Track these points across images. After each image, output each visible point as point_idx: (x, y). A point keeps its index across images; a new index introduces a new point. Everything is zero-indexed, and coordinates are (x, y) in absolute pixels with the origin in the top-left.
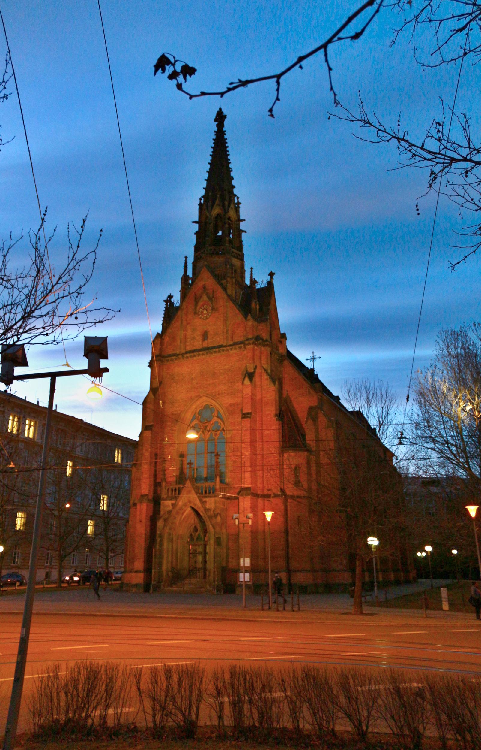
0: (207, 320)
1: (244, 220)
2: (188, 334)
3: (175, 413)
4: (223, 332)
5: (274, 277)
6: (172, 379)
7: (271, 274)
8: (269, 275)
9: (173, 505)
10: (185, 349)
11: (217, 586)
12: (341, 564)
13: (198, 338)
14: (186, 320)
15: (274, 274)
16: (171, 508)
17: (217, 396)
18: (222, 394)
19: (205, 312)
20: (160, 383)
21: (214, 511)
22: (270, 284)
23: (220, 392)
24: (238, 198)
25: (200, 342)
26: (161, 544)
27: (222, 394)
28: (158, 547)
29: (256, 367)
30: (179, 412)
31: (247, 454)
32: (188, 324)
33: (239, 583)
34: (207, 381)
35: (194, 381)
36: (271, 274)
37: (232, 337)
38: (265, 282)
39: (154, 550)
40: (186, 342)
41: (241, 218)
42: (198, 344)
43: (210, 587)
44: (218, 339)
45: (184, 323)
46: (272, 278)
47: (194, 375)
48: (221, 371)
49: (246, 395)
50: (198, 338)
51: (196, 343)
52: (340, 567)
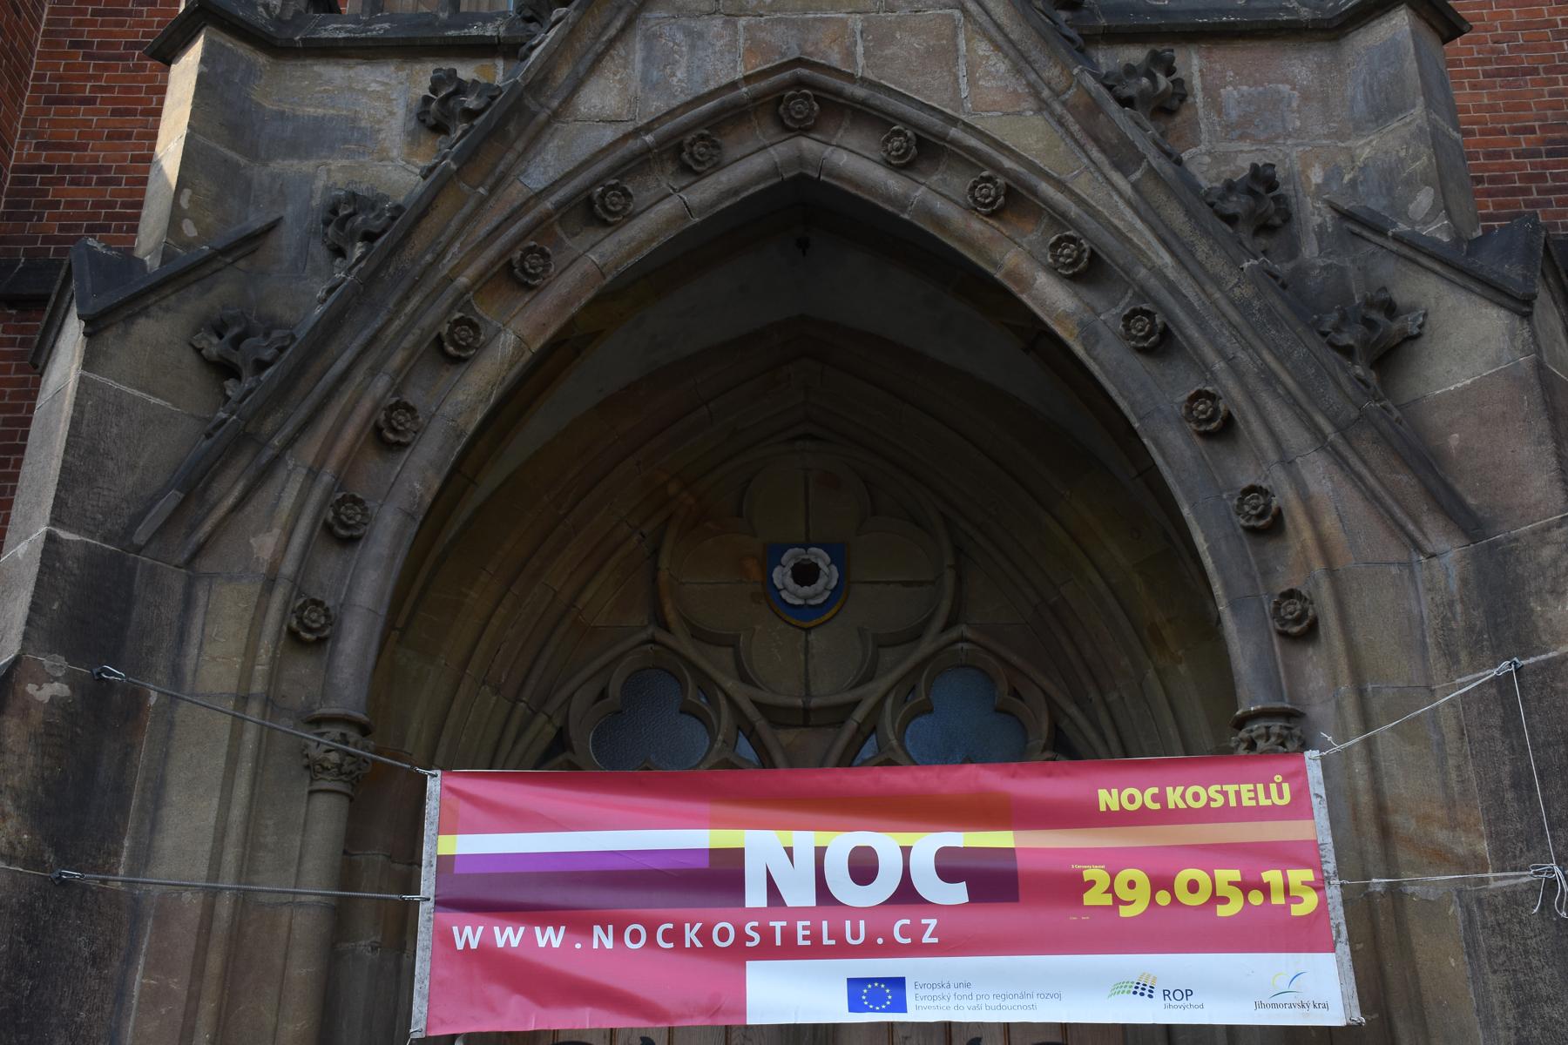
16: (397, 168)
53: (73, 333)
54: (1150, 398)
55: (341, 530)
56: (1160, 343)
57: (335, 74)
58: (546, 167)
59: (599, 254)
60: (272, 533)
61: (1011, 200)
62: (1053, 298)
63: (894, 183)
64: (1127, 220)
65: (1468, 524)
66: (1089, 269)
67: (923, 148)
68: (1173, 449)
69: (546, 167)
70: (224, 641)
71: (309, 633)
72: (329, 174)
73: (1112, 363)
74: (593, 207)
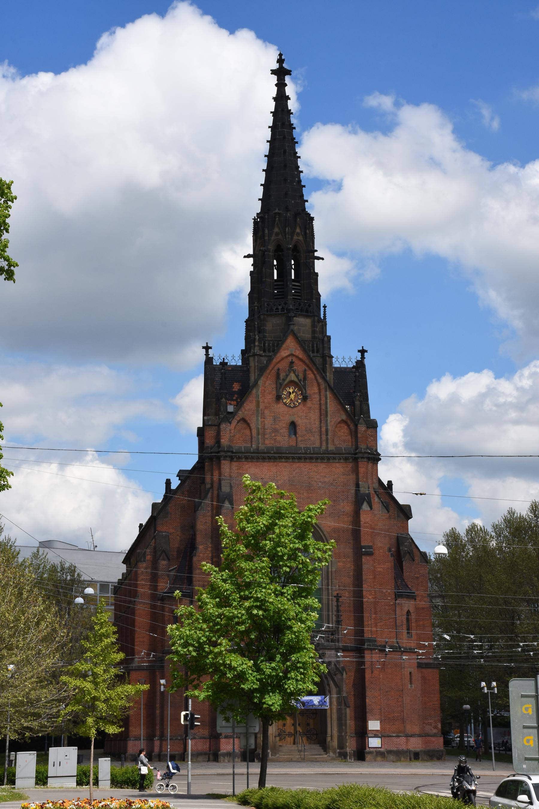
0: (295, 409)
1: (323, 259)
2: (266, 422)
7: (363, 352)
8: (359, 351)
10: (264, 443)
12: (435, 727)
13: (281, 431)
14: (263, 402)
15: (366, 351)
20: (231, 487)
21: (335, 665)
25: (286, 438)
31: (370, 597)
32: (266, 408)
33: (368, 750)
36: (363, 352)
37: (333, 441)
38: (354, 361)
41: (316, 254)
42: (284, 440)
44: (312, 438)
45: (262, 406)
46: (363, 357)
48: (320, 484)
49: (365, 523)
50: (281, 431)
51: (279, 438)
52: (435, 731)
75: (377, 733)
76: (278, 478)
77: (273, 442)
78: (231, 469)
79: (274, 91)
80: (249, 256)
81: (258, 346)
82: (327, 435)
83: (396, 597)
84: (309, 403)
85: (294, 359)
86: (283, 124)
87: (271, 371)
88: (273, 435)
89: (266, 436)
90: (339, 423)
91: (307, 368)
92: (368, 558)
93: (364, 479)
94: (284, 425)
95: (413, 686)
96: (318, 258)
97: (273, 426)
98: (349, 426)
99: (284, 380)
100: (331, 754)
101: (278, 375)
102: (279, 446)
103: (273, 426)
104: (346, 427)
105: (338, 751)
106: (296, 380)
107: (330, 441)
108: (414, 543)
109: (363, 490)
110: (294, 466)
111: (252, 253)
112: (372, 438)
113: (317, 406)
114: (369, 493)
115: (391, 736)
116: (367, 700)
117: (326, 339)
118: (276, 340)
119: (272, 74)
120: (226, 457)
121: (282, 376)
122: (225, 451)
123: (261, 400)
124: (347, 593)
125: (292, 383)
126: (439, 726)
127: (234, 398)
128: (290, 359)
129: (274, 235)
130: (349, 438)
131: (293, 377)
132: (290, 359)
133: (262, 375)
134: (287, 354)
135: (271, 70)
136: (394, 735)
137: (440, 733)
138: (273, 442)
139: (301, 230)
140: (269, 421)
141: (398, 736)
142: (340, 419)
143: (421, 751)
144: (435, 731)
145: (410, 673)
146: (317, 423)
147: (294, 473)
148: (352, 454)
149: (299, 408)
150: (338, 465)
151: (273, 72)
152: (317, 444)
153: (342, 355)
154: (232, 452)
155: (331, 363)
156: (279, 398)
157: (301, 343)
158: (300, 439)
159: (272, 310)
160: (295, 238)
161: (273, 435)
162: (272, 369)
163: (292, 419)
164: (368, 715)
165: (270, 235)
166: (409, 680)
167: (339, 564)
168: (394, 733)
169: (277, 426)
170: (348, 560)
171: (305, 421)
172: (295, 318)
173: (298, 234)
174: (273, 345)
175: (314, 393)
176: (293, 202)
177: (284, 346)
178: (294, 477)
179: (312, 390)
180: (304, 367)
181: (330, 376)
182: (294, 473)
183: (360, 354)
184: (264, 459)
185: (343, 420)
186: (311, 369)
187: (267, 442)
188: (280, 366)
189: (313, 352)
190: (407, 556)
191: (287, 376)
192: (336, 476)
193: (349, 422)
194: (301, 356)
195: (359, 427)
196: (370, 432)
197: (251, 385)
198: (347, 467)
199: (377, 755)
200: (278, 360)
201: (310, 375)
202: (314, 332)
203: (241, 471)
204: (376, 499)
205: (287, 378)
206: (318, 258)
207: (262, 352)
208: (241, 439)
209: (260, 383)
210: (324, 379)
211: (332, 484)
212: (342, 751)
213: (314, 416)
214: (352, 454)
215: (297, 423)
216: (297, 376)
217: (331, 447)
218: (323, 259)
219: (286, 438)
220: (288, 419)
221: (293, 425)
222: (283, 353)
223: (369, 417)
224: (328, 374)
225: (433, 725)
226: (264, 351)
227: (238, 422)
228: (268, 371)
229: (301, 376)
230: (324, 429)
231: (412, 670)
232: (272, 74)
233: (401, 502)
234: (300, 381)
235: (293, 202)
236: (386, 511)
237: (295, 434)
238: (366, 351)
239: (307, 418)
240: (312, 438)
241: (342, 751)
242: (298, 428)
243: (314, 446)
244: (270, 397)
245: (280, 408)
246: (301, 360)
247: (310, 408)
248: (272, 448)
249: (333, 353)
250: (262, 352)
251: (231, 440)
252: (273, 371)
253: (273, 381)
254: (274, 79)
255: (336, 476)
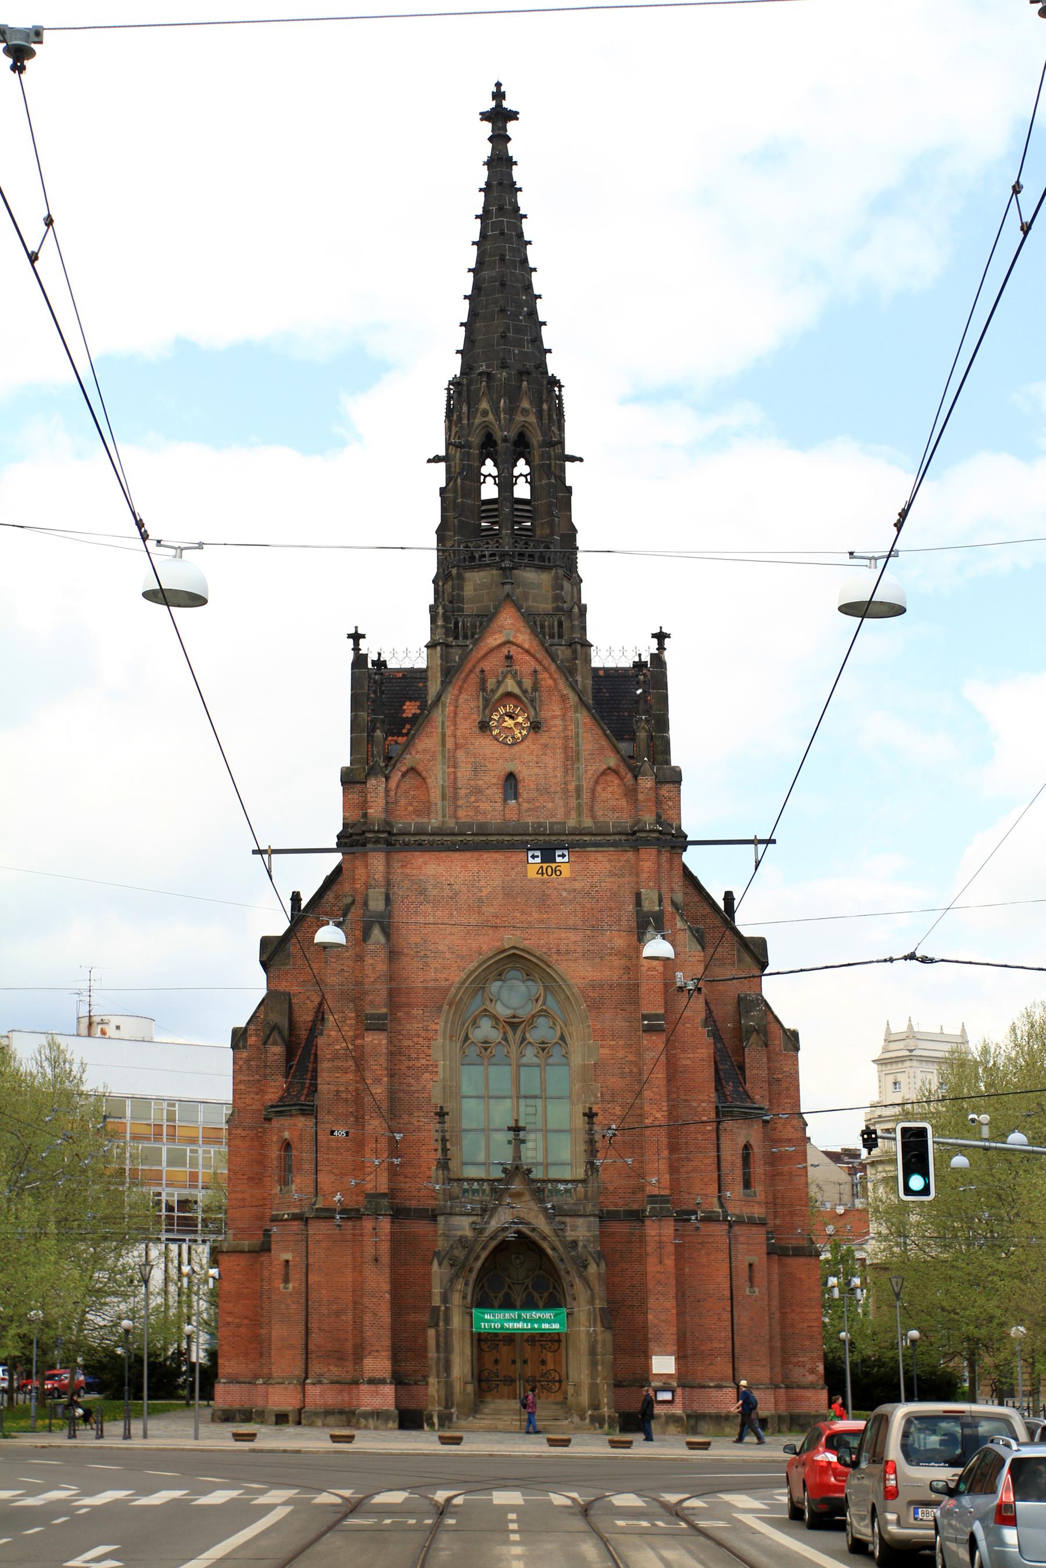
0: (516, 748)
1: (581, 460)
2: (459, 775)
3: (431, 984)
4: (565, 791)
5: (667, 642)
6: (421, 894)
7: (661, 637)
8: (654, 636)
9: (473, 1225)
10: (455, 816)
11: (609, 1417)
12: (812, 1371)
15: (668, 636)
16: (469, 1233)
17: (555, 957)
18: (567, 952)
19: (509, 723)
20: (388, 900)
22: (658, 660)
23: (563, 948)
24: (561, 387)
25: (499, 806)
26: (447, 1321)
27: (567, 952)
28: (441, 1324)
29: (660, 901)
30: (443, 984)
32: (457, 746)
34: (523, 913)
35: (484, 909)
36: (661, 637)
37: (592, 809)
39: (431, 1333)
40: (456, 797)
41: (569, 451)
42: (492, 810)
43: (582, 1418)
44: (550, 805)
46: (661, 648)
47: (484, 893)
48: (564, 894)
51: (483, 806)
52: (811, 1378)
53: (435, 1263)
54: (561, 1266)
55: (466, 1284)
56: (562, 1260)
57: (458, 1218)
58: (487, 1234)
59: (494, 1243)
60: (460, 1285)
61: (545, 1238)
62: (550, 1252)
63: (530, 1234)
64: (558, 1244)
65: (591, 1290)
66: (554, 1249)
67: (534, 1230)
68: (563, 1273)
69: (487, 1234)
70: (456, 1298)
71: (465, 1298)
72: (459, 1233)
73: (556, 1261)
74: (492, 1238)
75: (670, 1381)
76: (482, 883)
77: (472, 813)
78: (388, 864)
79: (486, 150)
80: (437, 459)
81: (443, 626)
82: (578, 797)
83: (717, 1115)
84: (544, 738)
85: (513, 650)
86: (501, 209)
87: (468, 675)
88: (473, 799)
89: (460, 802)
90: (603, 773)
91: (539, 668)
92: (654, 1038)
93: (651, 884)
94: (494, 780)
95: (756, 1290)
96: (573, 459)
97: (472, 783)
98: (622, 779)
99: (493, 691)
100: (576, 1419)
101: (483, 681)
102: (483, 820)
103: (472, 783)
104: (617, 782)
105: (590, 1412)
106: (517, 691)
107: (585, 810)
108: (772, 1012)
109: (650, 904)
110: (513, 859)
111: (442, 453)
112: (671, 804)
113: (559, 742)
114: (662, 912)
115: (704, 1387)
116: (650, 1317)
117: (576, 610)
118: (478, 616)
119: (481, 120)
120: (377, 841)
121: (491, 683)
122: (374, 832)
123: (449, 732)
124: (618, 1108)
125: (509, 695)
126: (821, 1368)
127: (405, 731)
128: (505, 651)
129: (479, 415)
130: (623, 803)
131: (510, 685)
132: (505, 651)
133: (450, 683)
134: (499, 642)
135: (481, 114)
136: (712, 1384)
137: (822, 1382)
138: (472, 813)
139: (531, 403)
140: (464, 772)
141: (719, 1387)
142: (605, 767)
143: (772, 1416)
144: (811, 1378)
145: (751, 1265)
146: (560, 775)
147: (514, 873)
148: (628, 834)
149: (523, 746)
150: (599, 856)
151: (485, 116)
152: (559, 817)
153: (613, 641)
154: (390, 833)
155: (588, 659)
156: (484, 726)
157: (531, 619)
158: (525, 806)
159: (472, 558)
160: (519, 418)
161: (473, 799)
162: (471, 671)
163: (511, 767)
164: (653, 1346)
165: (471, 415)
166: (747, 1279)
167: (603, 1051)
168: (712, 1379)
169: (480, 782)
170: (621, 1043)
171: (536, 770)
172: (516, 572)
173: (525, 412)
174: (474, 626)
175: (554, 717)
176: (516, 351)
177: (494, 626)
178: (513, 881)
179: (552, 711)
180: (533, 664)
181: (585, 682)
182: (514, 873)
183: (655, 641)
184: (451, 848)
185: (609, 768)
186: (546, 669)
187: (461, 813)
188: (486, 665)
189: (552, 636)
190: (754, 1037)
191: (499, 683)
192: (596, 879)
193: (623, 770)
194: (527, 646)
195: (640, 782)
196: (665, 790)
197: (429, 702)
198: (619, 860)
199: (667, 1423)
200: (482, 653)
201: (546, 681)
202: (557, 598)
203: (408, 871)
204: (679, 924)
205: (498, 687)
206: (573, 459)
207: (451, 639)
208: (410, 808)
209: (448, 698)
210: (573, 686)
211: (588, 893)
212: (596, 1413)
213: (554, 761)
214: (628, 834)
215: (520, 777)
216: (519, 684)
217: (588, 823)
218: (581, 460)
219: (499, 804)
220: (503, 767)
221: (511, 779)
222: (493, 640)
223: (668, 761)
224: (579, 678)
225: (808, 1366)
226: (456, 638)
227: (404, 775)
228: (463, 675)
229: (528, 683)
230: (572, 787)
231: (754, 1259)
232: (481, 120)
233: (746, 932)
234: (525, 692)
235: (516, 351)
236: (699, 947)
237: (516, 796)
238: (668, 636)
239: (539, 764)
240: (550, 805)
241: (596, 1413)
242: (520, 786)
243: (554, 820)
244: (467, 726)
245: (485, 746)
246: (527, 652)
247: (546, 746)
248: (470, 826)
249: (590, 638)
250: (451, 639)
251: (387, 810)
252: (472, 676)
253: (472, 695)
254: (487, 128)
255: (596, 879)
